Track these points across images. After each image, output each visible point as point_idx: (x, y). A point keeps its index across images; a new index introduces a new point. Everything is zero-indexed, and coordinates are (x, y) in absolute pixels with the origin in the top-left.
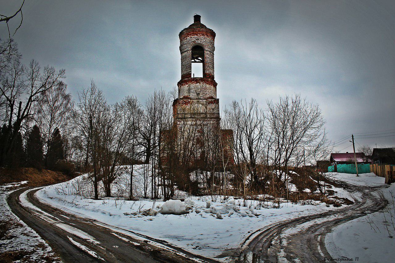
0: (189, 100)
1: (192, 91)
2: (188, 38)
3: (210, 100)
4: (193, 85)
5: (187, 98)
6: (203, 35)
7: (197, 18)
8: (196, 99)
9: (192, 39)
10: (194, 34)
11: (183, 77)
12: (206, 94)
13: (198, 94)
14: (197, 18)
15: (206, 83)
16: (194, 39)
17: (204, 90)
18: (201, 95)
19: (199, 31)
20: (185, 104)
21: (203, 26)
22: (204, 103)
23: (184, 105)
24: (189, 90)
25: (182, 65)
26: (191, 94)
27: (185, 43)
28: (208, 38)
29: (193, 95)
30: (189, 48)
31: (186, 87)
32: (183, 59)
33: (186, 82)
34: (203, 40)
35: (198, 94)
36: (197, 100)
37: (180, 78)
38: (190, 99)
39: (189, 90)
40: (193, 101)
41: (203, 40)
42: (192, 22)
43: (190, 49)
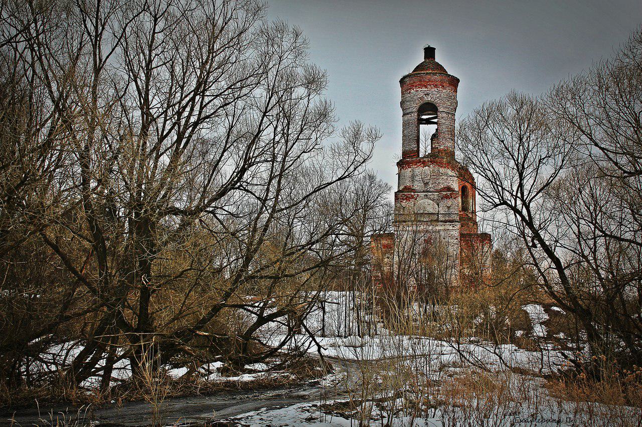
0: (413, 194)
1: (417, 178)
2: (412, 91)
3: (444, 193)
4: (419, 170)
5: (409, 189)
6: (436, 86)
7: (430, 52)
8: (424, 192)
9: (420, 94)
10: (421, 86)
11: (405, 154)
12: (439, 183)
13: (426, 184)
14: (430, 52)
15: (439, 166)
16: (421, 95)
17: (435, 177)
18: (430, 186)
19: (430, 81)
20: (406, 199)
21: (440, 68)
22: (436, 197)
23: (405, 201)
24: (413, 177)
25: (404, 136)
26: (416, 183)
27: (408, 99)
28: (444, 91)
29: (418, 186)
30: (414, 107)
31: (408, 172)
32: (406, 125)
33: (409, 164)
34: (434, 95)
35: (426, 184)
36: (425, 194)
37: (400, 156)
38: (414, 191)
39: (413, 177)
40: (418, 195)
41: (434, 95)
42: (421, 59)
43: (415, 110)
